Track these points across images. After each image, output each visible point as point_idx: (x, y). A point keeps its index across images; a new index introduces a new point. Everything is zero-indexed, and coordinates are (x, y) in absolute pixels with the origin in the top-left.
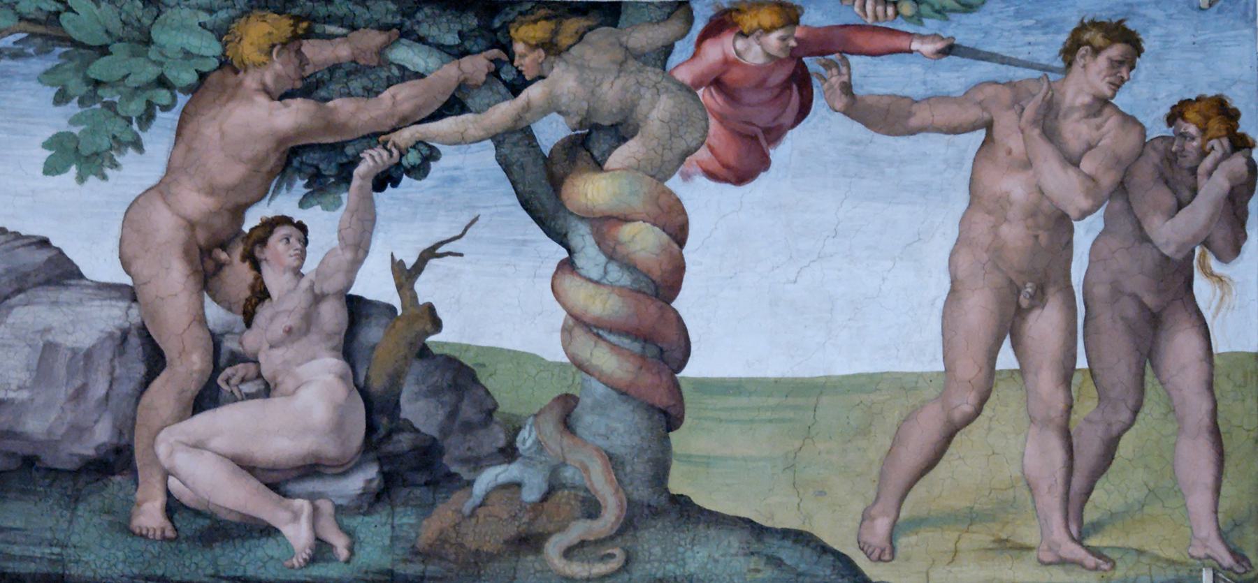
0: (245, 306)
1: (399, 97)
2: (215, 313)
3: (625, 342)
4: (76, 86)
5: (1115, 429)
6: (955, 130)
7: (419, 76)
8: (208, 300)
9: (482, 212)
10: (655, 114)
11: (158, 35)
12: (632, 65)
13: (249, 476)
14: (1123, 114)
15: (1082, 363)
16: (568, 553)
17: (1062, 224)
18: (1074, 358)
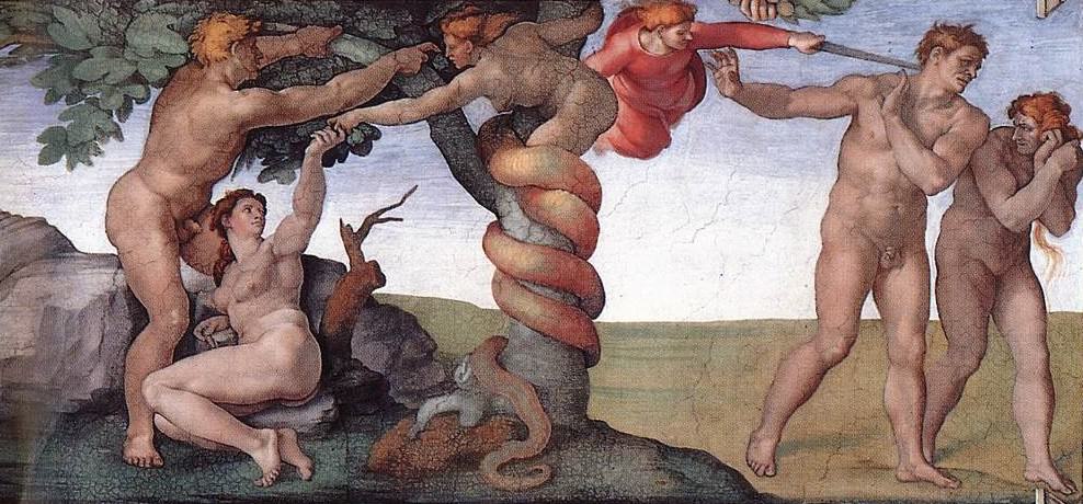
1: (344, 85)
6: (826, 116)
7: (360, 66)
10: (570, 98)
11: (135, 38)
15: (934, 316)
17: (917, 198)
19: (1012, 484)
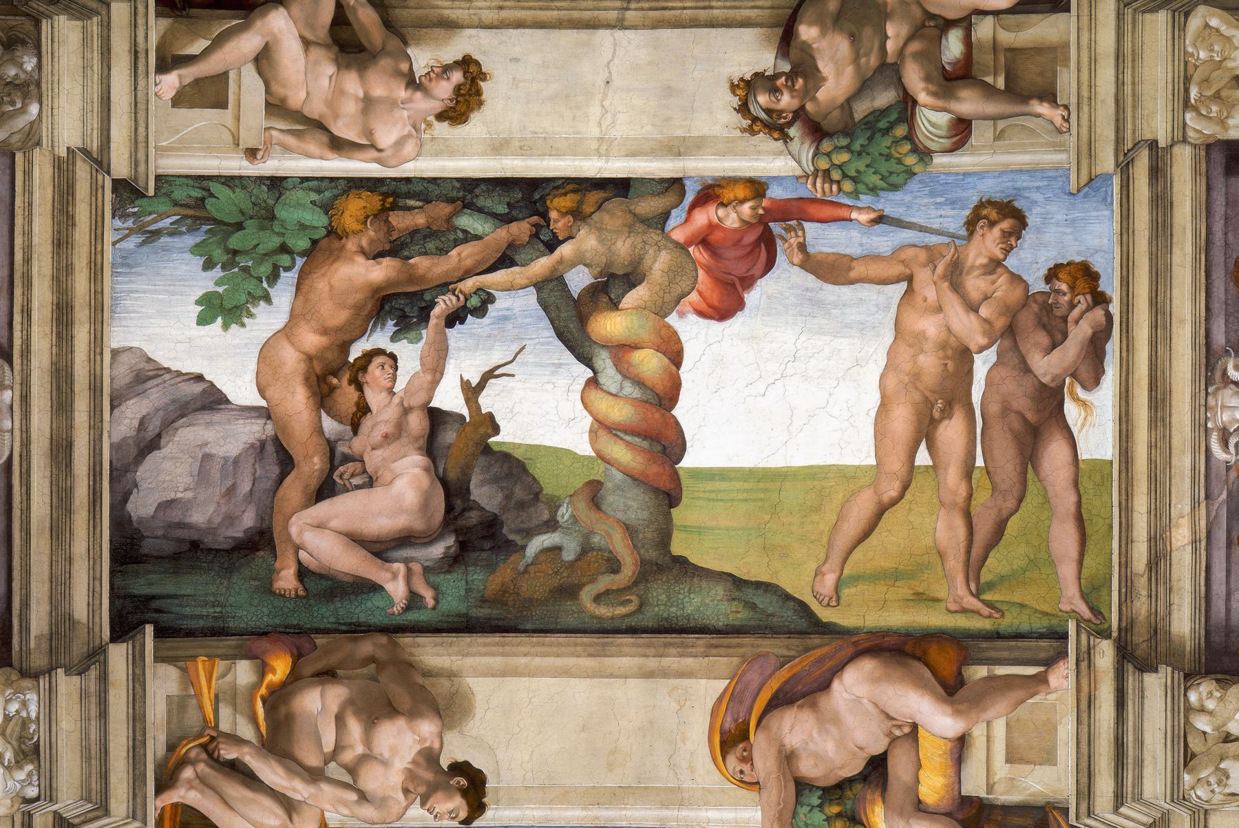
0: (352, 419)
2: (329, 425)
3: (637, 440)
4: (219, 255)
5: (1005, 513)
7: (478, 238)
8: (324, 415)
9: (527, 342)
11: (282, 213)
12: (640, 227)
13: (358, 547)
14: (1012, 274)
15: (980, 462)
16: (597, 599)
17: (964, 356)
18: (974, 459)
19: (1048, 614)
